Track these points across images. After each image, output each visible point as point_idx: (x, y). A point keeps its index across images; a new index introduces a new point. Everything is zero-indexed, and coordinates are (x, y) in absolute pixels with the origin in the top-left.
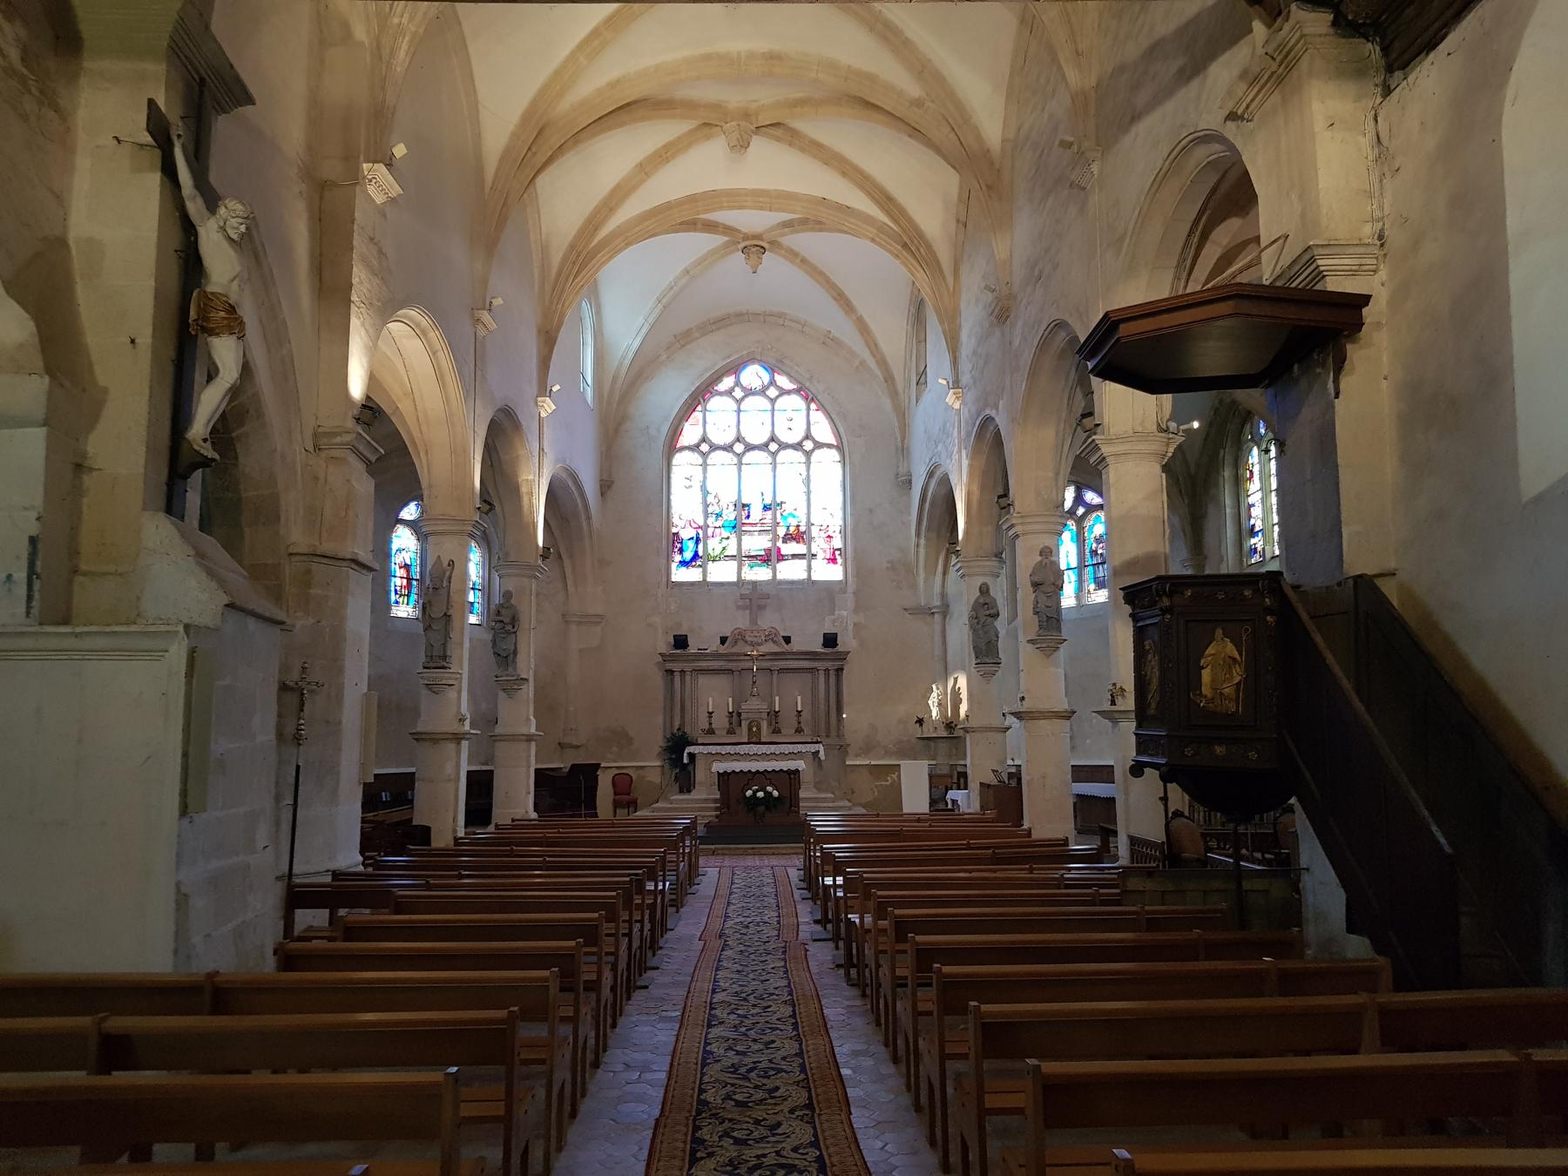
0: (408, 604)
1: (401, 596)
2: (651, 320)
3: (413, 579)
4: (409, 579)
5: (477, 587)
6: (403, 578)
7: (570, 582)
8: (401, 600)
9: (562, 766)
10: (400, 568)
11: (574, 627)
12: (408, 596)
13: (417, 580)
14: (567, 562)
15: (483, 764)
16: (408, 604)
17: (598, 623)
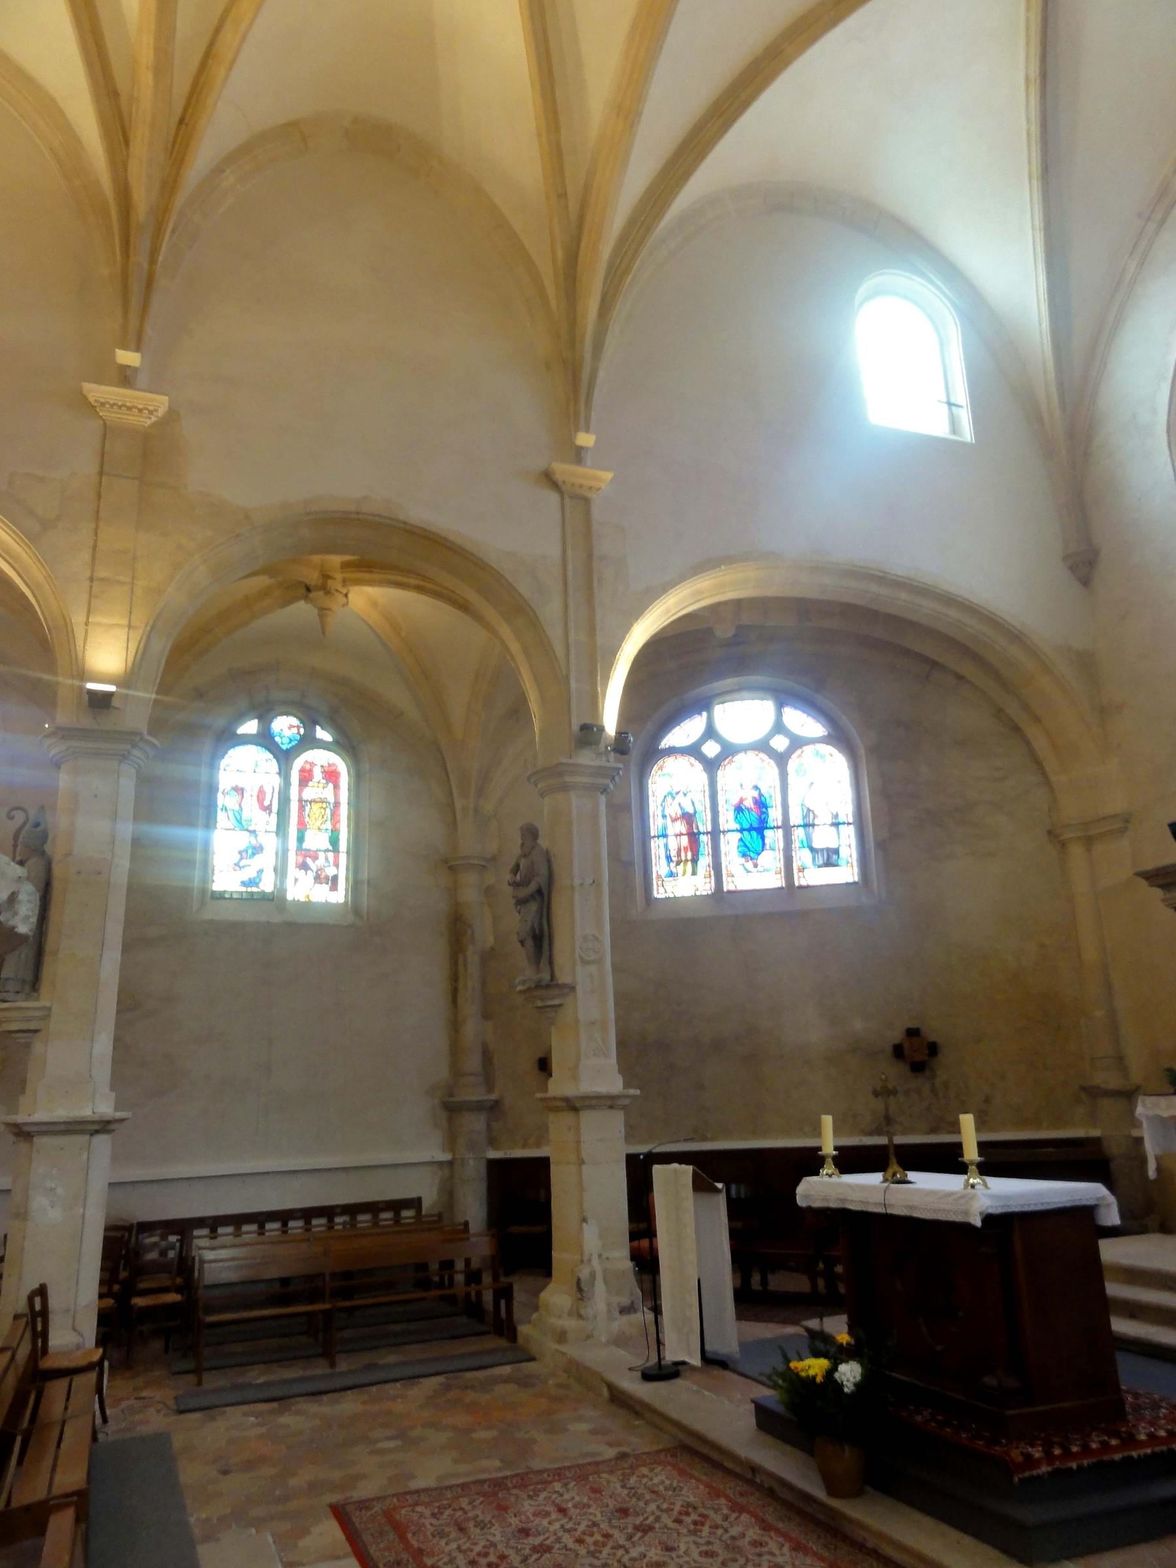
0: (694, 873)
1: (678, 863)
2: (1038, 222)
3: (699, 833)
4: (693, 837)
5: (841, 820)
6: (681, 834)
7: (1051, 764)
8: (681, 868)
9: (1095, 1133)
10: (674, 820)
11: (1076, 851)
12: (695, 861)
13: (707, 833)
14: (1032, 732)
15: (871, 1133)
16: (694, 873)
17: (1123, 831)
